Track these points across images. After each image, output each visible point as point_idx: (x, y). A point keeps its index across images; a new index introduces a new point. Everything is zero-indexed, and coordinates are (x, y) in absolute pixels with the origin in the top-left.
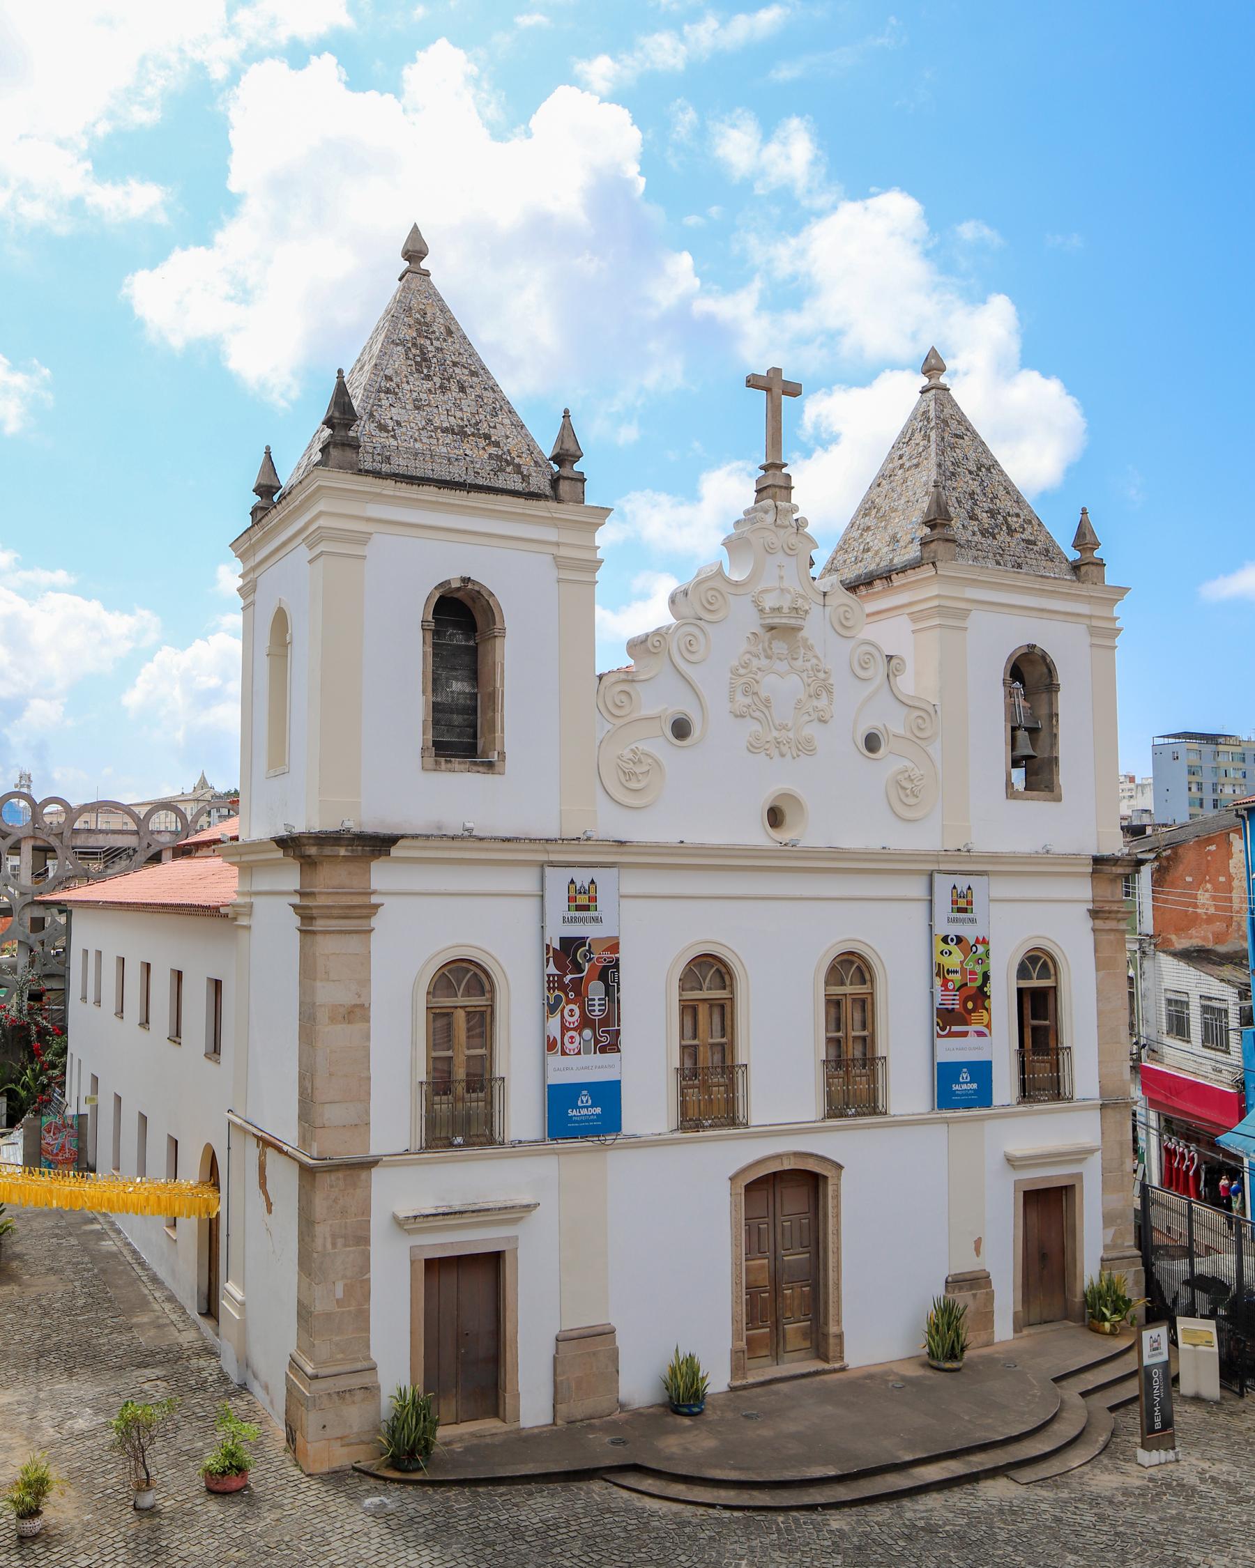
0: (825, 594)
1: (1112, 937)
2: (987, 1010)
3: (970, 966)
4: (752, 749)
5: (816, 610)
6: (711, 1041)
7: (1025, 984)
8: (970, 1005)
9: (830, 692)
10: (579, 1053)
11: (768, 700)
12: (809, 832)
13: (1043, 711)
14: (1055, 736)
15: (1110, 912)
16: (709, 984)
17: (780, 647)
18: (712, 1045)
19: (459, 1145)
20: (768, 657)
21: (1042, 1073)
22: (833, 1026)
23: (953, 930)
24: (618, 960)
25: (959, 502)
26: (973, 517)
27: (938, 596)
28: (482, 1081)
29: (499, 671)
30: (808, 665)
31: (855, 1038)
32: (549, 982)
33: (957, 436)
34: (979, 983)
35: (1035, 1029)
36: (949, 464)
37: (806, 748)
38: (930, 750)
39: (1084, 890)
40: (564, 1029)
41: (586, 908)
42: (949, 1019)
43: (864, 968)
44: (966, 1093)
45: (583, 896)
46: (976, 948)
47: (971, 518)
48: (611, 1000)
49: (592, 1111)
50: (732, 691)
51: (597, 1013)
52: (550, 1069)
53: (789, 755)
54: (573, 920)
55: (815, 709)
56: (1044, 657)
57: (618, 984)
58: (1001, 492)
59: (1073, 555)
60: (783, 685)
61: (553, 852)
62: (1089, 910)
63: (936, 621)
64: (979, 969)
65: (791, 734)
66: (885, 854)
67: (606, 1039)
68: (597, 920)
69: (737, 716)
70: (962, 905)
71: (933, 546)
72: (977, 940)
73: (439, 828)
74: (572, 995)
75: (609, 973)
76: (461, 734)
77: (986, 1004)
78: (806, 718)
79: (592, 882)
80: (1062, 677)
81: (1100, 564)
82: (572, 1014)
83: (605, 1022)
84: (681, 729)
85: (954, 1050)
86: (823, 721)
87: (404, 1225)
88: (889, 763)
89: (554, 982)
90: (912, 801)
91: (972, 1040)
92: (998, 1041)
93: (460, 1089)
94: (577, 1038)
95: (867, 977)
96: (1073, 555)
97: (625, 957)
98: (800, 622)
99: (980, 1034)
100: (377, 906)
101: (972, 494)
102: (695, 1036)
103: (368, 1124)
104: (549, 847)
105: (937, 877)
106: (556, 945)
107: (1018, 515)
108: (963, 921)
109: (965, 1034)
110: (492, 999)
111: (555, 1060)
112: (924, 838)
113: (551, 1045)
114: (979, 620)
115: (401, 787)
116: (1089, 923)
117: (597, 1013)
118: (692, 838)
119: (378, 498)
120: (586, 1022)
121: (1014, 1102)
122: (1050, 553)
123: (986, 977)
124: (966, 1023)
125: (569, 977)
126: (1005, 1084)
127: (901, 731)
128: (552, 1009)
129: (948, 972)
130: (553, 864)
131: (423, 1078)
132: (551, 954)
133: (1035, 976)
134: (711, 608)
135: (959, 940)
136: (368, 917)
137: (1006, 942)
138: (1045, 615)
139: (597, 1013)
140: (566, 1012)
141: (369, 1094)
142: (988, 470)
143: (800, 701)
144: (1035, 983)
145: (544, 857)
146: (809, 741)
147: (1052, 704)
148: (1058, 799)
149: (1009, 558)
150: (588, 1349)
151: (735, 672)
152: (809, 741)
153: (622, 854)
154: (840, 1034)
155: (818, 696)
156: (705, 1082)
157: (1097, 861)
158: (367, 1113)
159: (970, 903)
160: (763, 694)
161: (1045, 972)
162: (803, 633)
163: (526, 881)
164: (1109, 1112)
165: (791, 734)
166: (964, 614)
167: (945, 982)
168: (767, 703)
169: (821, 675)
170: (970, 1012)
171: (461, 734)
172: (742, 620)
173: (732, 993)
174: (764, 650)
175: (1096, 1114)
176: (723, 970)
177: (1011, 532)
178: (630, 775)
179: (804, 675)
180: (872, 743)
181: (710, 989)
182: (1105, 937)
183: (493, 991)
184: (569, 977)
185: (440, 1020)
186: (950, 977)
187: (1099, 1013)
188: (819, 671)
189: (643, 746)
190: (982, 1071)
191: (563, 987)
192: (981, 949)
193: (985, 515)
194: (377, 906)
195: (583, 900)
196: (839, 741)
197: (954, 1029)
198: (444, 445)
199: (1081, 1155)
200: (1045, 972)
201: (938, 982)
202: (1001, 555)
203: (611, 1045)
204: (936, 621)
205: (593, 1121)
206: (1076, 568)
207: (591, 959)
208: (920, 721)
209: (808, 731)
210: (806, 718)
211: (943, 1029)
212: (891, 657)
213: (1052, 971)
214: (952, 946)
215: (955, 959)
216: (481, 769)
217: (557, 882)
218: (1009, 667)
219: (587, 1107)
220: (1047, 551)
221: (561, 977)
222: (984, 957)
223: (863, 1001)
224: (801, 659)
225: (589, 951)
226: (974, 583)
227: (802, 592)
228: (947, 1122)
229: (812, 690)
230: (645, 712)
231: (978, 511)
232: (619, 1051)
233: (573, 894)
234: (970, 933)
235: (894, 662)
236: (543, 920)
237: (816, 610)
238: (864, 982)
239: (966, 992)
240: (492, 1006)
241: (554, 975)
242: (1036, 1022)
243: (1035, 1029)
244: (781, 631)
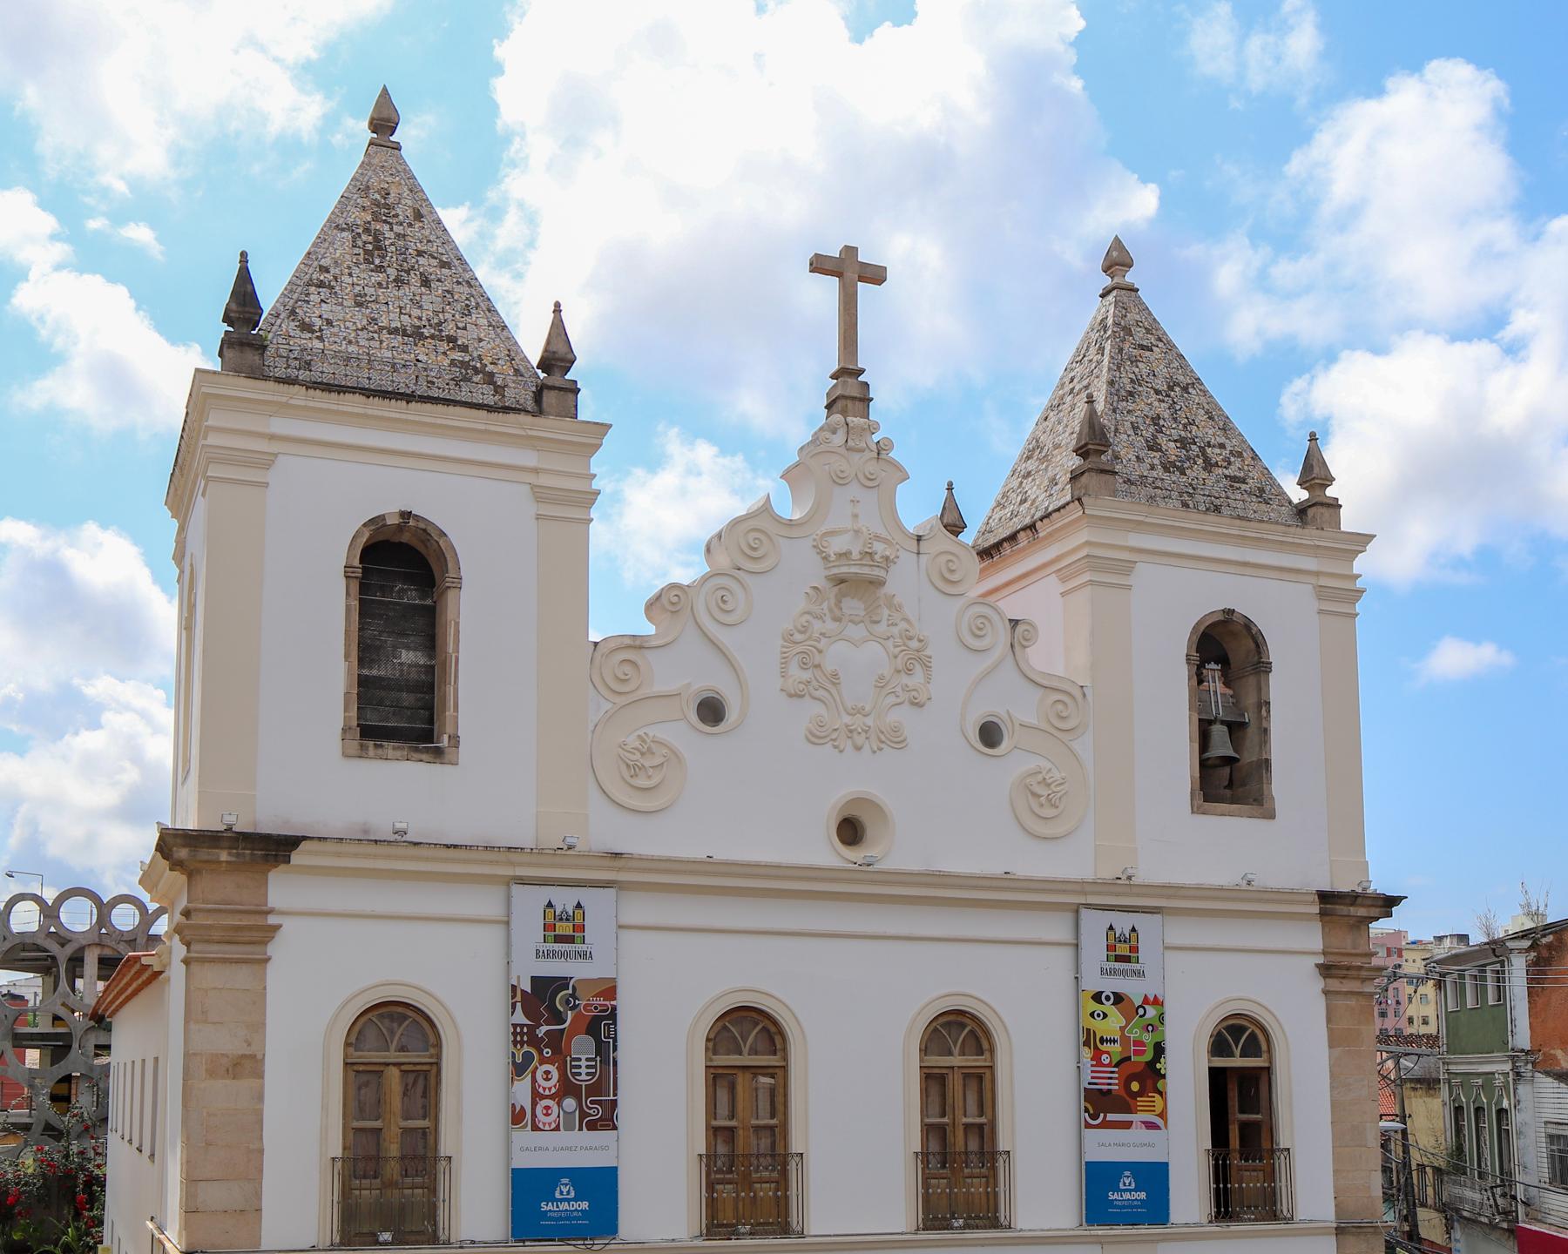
0: (919, 538)
1: (1352, 1002)
2: (1161, 1093)
3: (1135, 1033)
4: (814, 738)
5: (906, 560)
6: (754, 1122)
7: (1220, 1062)
8: (1135, 1086)
9: (927, 667)
10: (557, 1129)
11: (835, 675)
12: (898, 849)
13: (1250, 700)
14: (1266, 732)
15: (1348, 968)
16: (747, 1049)
17: (853, 606)
18: (757, 1128)
19: (386, 1243)
20: (837, 619)
21: (1248, 1181)
22: (935, 1107)
23: (1109, 985)
24: (614, 1008)
25: (1135, 428)
26: (1153, 446)
27: (1088, 543)
29: (452, 631)
30: (895, 630)
31: (967, 1126)
32: (515, 1034)
33: (1142, 347)
34: (1148, 1056)
35: (1245, 1127)
36: (1126, 381)
37: (895, 739)
38: (1076, 745)
40: (536, 1096)
41: (569, 939)
42: (1101, 1104)
43: (980, 1034)
44: (1130, 1204)
45: (565, 924)
46: (1147, 1012)
47: (1150, 448)
48: (605, 1062)
49: (576, 1205)
50: (785, 662)
51: (584, 1077)
52: (515, 1147)
53: (867, 747)
54: (552, 955)
55: (906, 688)
56: (1248, 625)
57: (615, 1040)
58: (1201, 417)
59: (1298, 495)
60: (858, 656)
61: (521, 865)
62: (1317, 966)
63: (1086, 577)
64: (1149, 1039)
65: (869, 721)
66: (1007, 881)
67: (596, 1112)
68: (585, 955)
69: (791, 696)
70: (1123, 952)
71: (1084, 479)
72: (1146, 1000)
73: (366, 832)
74: (547, 1052)
75: (601, 1027)
77: (1160, 1085)
78: (892, 699)
79: (579, 906)
80: (1276, 652)
81: (1334, 505)
82: (548, 1076)
83: (597, 1089)
84: (711, 711)
85: (1111, 1146)
86: (920, 705)
88: (1013, 762)
89: (522, 1033)
90: (1048, 812)
91: (1138, 1134)
92: (1181, 1136)
93: (392, 1169)
94: (555, 1108)
95: (985, 1045)
96: (1298, 495)
97: (625, 1004)
98: (882, 573)
99: (1150, 1126)
100: (278, 927)
101: (1156, 420)
102: (732, 1116)
103: (259, 1210)
104: (513, 856)
105: (1083, 912)
106: (526, 986)
107: (1222, 446)
108: (1124, 973)
109: (1127, 1125)
110: (439, 1056)
111: (524, 1136)
112: (1072, 862)
113: (517, 1117)
114: (1147, 575)
115: (316, 776)
116: (1319, 983)
117: (584, 1077)
119: (284, 409)
120: (567, 1088)
121: (1205, 1220)
122: (1267, 492)
123: (1159, 1050)
124: (1129, 1110)
125: (544, 1028)
126: (1190, 1193)
127: (1034, 721)
128: (519, 1069)
129: (1102, 1040)
130: (523, 881)
131: (338, 1153)
132: (519, 998)
133: (1238, 1052)
134: (754, 554)
135: (1118, 999)
136: (265, 943)
137: (1190, 998)
138: (1248, 571)
139: (584, 1077)
140: (539, 1074)
141: (261, 1171)
142: (1185, 389)
143: (882, 677)
144: (1237, 1062)
145: (510, 872)
146: (896, 730)
147: (1261, 688)
148: (1271, 815)
149: (1202, 499)
151: (788, 638)
152: (896, 730)
153: (620, 870)
154: (945, 1120)
155: (909, 671)
156: (746, 1176)
157: (1325, 897)
158: (258, 1195)
159: (1135, 949)
160: (829, 667)
161: (1252, 1048)
162: (888, 589)
163: (487, 903)
164: (1350, 1239)
165: (869, 721)
166: (1127, 568)
167: (1097, 1057)
168: (835, 675)
169: (914, 644)
170: (1134, 1095)
173: (785, 1058)
174: (831, 610)
175: (1332, 1241)
176: (773, 1029)
177: (1209, 465)
178: (636, 769)
179: (890, 643)
180: (990, 735)
181: (754, 1051)
182: (1340, 1002)
183: (438, 1045)
184: (544, 1028)
185: (362, 1079)
186: (1105, 1047)
187: (1335, 1105)
188: (910, 638)
189: (655, 732)
190: (1154, 1177)
191: (535, 1041)
192: (1151, 1012)
193: (1172, 445)
194: (278, 927)
195: (564, 928)
196: (942, 730)
197: (1110, 1117)
200: (1252, 1048)
201: (1087, 1054)
202: (1190, 495)
204: (1086, 577)
205: (578, 1218)
206: (1301, 511)
207: (575, 1007)
208: (1060, 707)
209: (894, 717)
210: (892, 699)
211: (1094, 1117)
212: (1017, 622)
213: (1264, 1047)
214: (1108, 1007)
215: (1113, 1023)
216: (424, 757)
217: (530, 906)
218: (1196, 639)
219: (568, 1200)
220: (1262, 490)
221: (532, 1030)
222: (1156, 1023)
223: (980, 1078)
224: (884, 622)
225: (573, 995)
226: (1139, 526)
227: (884, 534)
228: (1099, 1241)
229: (899, 663)
230: (659, 687)
231: (1162, 440)
232: (615, 1128)
233: (550, 920)
234: (1134, 990)
235: (1020, 628)
236: (508, 954)
237: (906, 560)
238: (980, 1052)
239: (1128, 1069)
240: (438, 1065)
241: (522, 1026)
242: (1245, 1117)
243: (1245, 1127)
244: (855, 584)
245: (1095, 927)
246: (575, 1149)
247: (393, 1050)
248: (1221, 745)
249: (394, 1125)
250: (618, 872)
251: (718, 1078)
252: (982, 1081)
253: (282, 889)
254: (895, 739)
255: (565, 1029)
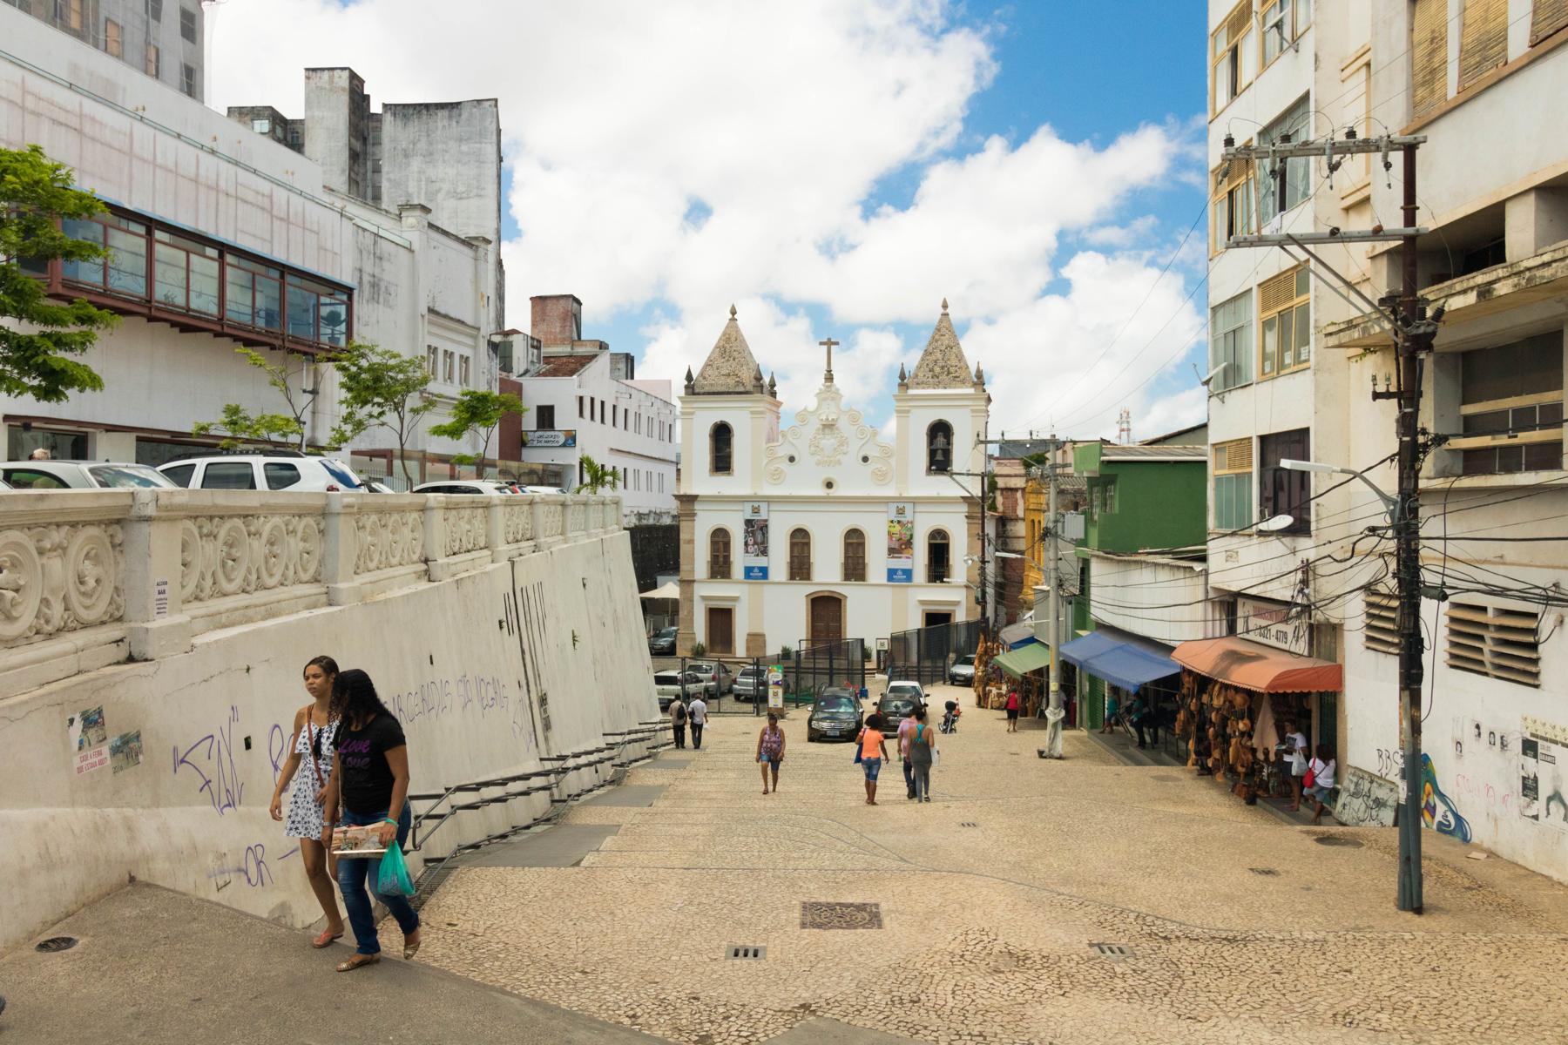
4: (818, 464)
28: (727, 562)
37: (839, 463)
39: (964, 508)
42: (892, 551)
60: (828, 442)
70: (901, 512)
76: (722, 462)
84: (792, 459)
87: (704, 598)
88: (871, 465)
112: (890, 491)
118: (794, 493)
150: (756, 639)
171: (722, 462)
172: (815, 424)
180: (865, 459)
185: (714, 543)
190: (908, 574)
198: (722, 380)
199: (957, 603)
203: (764, 552)
215: (897, 528)
245: (893, 508)
246: (761, 561)
247: (720, 539)
248: (939, 457)
249: (721, 554)
250: (769, 500)
251: (793, 545)
252: (861, 545)
253: (697, 506)
254: (839, 463)
255: (757, 531)
